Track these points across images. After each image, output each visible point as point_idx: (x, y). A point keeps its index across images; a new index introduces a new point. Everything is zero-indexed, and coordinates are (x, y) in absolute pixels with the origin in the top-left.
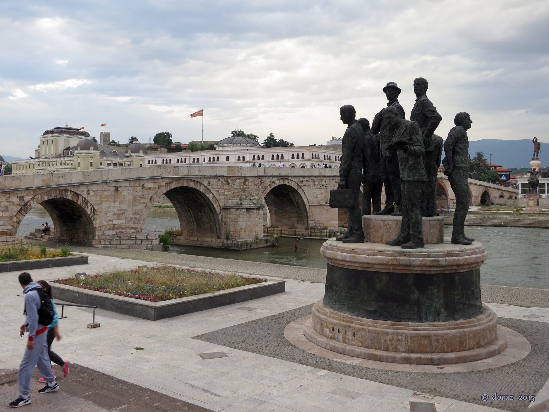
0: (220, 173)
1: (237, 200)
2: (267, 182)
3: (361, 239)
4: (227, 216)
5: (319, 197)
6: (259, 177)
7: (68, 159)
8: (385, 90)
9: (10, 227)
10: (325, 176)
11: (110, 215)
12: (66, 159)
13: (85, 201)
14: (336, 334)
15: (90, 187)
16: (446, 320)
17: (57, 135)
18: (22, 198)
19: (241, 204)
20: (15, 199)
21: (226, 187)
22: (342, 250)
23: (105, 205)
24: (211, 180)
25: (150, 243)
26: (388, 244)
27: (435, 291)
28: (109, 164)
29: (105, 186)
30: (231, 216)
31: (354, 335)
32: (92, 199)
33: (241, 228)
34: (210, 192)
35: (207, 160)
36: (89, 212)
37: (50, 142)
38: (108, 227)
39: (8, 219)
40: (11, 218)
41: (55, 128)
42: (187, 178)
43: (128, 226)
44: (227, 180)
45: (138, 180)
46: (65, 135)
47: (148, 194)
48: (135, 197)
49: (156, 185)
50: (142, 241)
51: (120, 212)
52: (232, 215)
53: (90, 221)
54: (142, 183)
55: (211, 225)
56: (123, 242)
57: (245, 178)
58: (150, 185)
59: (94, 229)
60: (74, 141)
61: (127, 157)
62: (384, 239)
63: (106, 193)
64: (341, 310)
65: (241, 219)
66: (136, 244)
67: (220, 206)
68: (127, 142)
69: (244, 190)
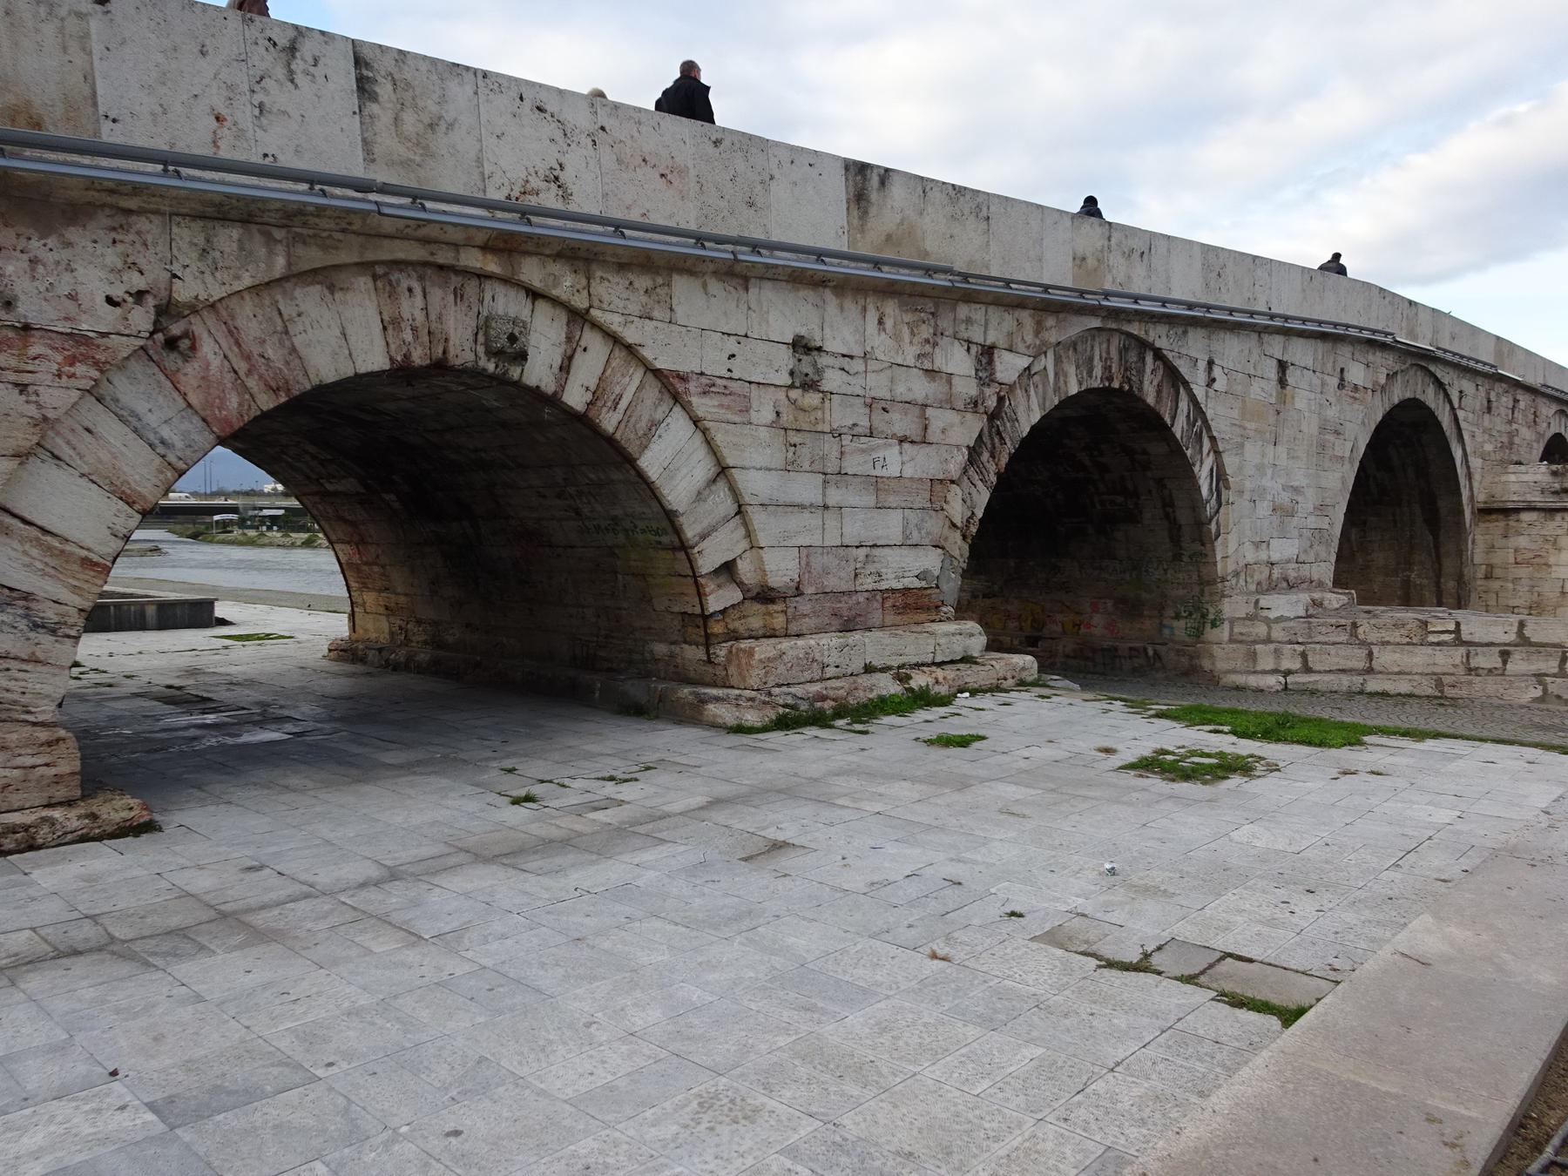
4: (1499, 542)
9: (931, 561)
20: (958, 362)
30: (1522, 542)
32: (1220, 415)
33: (1563, 593)
36: (1205, 491)
38: (1257, 577)
39: (921, 500)
43: (1305, 571)
48: (1323, 429)
50: (1505, 655)
51: (1285, 498)
52: (1528, 534)
53: (1190, 535)
55: (1407, 583)
56: (1384, 658)
59: (1208, 584)
66: (1469, 670)
67: (1472, 497)
69: (1511, 443)
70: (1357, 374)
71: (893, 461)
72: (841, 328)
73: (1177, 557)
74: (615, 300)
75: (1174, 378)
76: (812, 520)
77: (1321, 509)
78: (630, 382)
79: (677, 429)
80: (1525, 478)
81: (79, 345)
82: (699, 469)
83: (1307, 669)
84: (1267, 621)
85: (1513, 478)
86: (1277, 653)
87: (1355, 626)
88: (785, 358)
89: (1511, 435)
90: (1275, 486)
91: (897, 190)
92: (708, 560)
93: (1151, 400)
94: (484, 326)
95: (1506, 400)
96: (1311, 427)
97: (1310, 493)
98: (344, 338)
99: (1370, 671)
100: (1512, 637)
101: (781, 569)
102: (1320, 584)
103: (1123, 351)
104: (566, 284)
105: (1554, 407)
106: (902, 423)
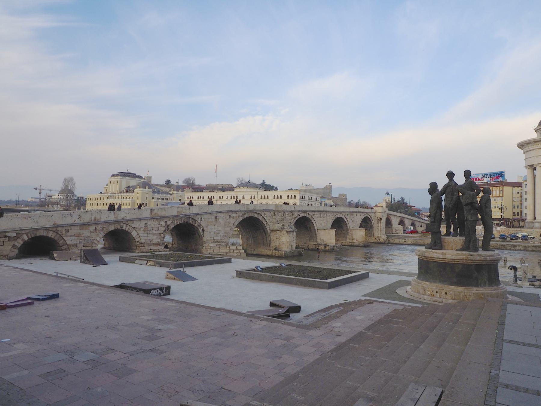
0: (271, 208)
1: (280, 225)
2: (296, 214)
3: (441, 248)
5: (323, 224)
6: (292, 211)
7: (130, 195)
8: (447, 175)
9: (159, 240)
10: (326, 212)
11: (212, 233)
12: (128, 194)
13: (199, 224)
14: (435, 294)
15: (202, 216)
16: (489, 286)
20: (163, 223)
21: (274, 217)
22: (436, 253)
23: (210, 227)
24: (266, 213)
26: (457, 250)
27: (484, 273)
28: (158, 199)
29: (210, 215)
31: (446, 293)
32: (203, 223)
34: (266, 221)
35: (229, 198)
37: (116, 182)
40: (160, 234)
42: (253, 211)
44: (274, 212)
45: (227, 212)
47: (233, 221)
49: (237, 216)
53: (201, 237)
54: (230, 214)
56: (221, 251)
57: (284, 212)
58: (234, 215)
60: (133, 182)
61: (171, 194)
62: (454, 248)
63: (210, 220)
64: (435, 282)
65: (283, 238)
68: (164, 183)
69: (283, 219)
71: (155, 232)
72: (149, 222)
74: (130, 223)
81: (99, 230)
82: (136, 234)
91: (155, 211)
92: (137, 240)
98: (112, 228)
101: (143, 241)
104: (126, 223)
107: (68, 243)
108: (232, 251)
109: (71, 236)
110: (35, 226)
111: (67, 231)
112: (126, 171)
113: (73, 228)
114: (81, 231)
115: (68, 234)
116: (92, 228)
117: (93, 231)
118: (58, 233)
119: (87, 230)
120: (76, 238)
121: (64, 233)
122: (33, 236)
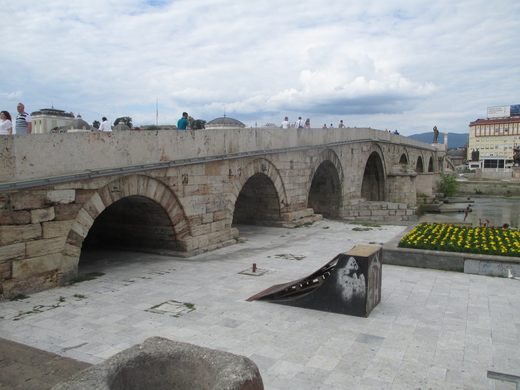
17: (45, 116)
18: (311, 158)
19: (406, 171)
20: (308, 160)
25: (404, 214)
30: (397, 183)
37: (38, 122)
41: (42, 110)
46: (53, 116)
48: (359, 162)
50: (396, 212)
52: (398, 182)
55: (372, 194)
56: (374, 213)
59: (340, 199)
60: (61, 122)
65: (406, 187)
66: (390, 215)
70: (365, 149)
73: (334, 192)
75: (336, 156)
76: (292, 191)
77: (359, 179)
78: (274, 171)
79: (278, 178)
80: (397, 168)
82: (280, 184)
83: (359, 216)
84: (351, 206)
85: (394, 168)
86: (354, 212)
87: (368, 206)
88: (289, 164)
89: (394, 156)
90: (352, 176)
92: (281, 201)
93: (332, 161)
94: (262, 166)
95: (393, 148)
96: (357, 162)
97: (357, 176)
98: (251, 172)
99: (371, 215)
100: (397, 208)
102: (359, 196)
103: (328, 152)
105: (403, 147)
106: (302, 173)
107: (189, 213)
108: (392, 213)
109: (193, 194)
110: (123, 163)
111: (185, 182)
112: (50, 108)
113: (195, 168)
114: (208, 181)
115: (188, 189)
116: (224, 170)
117: (226, 178)
118: (167, 187)
119: (218, 178)
120: (201, 197)
121: (180, 184)
122: (117, 198)
